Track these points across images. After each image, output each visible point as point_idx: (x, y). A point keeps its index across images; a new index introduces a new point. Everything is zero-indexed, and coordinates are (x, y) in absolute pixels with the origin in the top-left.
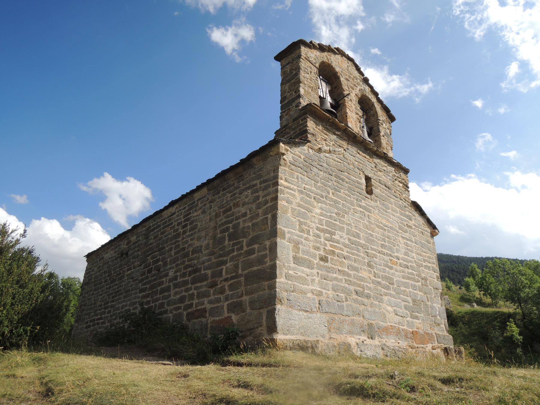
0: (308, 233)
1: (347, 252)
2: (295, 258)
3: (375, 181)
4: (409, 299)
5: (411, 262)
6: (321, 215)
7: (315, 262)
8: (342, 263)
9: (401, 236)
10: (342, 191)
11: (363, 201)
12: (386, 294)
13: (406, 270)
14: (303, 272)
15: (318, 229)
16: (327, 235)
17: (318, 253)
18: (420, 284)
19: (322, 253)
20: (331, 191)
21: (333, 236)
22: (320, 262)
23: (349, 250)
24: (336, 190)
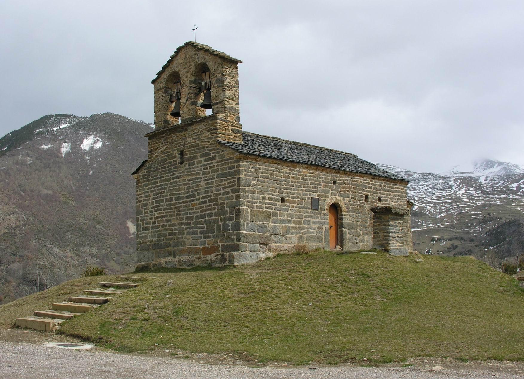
0: (147, 213)
1: (166, 213)
2: (143, 228)
3: (186, 150)
4: (205, 225)
5: (210, 196)
6: (154, 199)
7: (150, 226)
8: (163, 221)
9: (204, 180)
10: (164, 176)
11: (176, 173)
12: (186, 228)
13: (205, 205)
14: (146, 233)
15: (152, 208)
16: (156, 209)
17: (151, 221)
18: (216, 210)
19: (154, 220)
20: (158, 180)
21: (159, 208)
22: (153, 225)
23: (166, 211)
24: (160, 178)
